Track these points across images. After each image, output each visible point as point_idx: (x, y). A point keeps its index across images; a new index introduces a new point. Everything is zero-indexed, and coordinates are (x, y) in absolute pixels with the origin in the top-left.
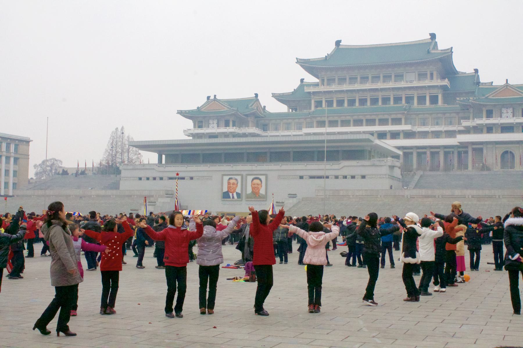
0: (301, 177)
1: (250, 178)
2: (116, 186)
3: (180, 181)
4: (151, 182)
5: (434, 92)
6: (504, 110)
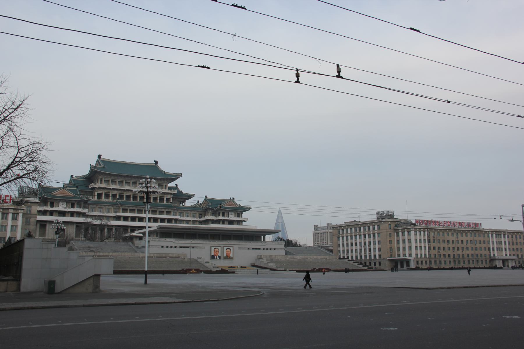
0: (248, 249)
3: (192, 249)
4: (169, 249)
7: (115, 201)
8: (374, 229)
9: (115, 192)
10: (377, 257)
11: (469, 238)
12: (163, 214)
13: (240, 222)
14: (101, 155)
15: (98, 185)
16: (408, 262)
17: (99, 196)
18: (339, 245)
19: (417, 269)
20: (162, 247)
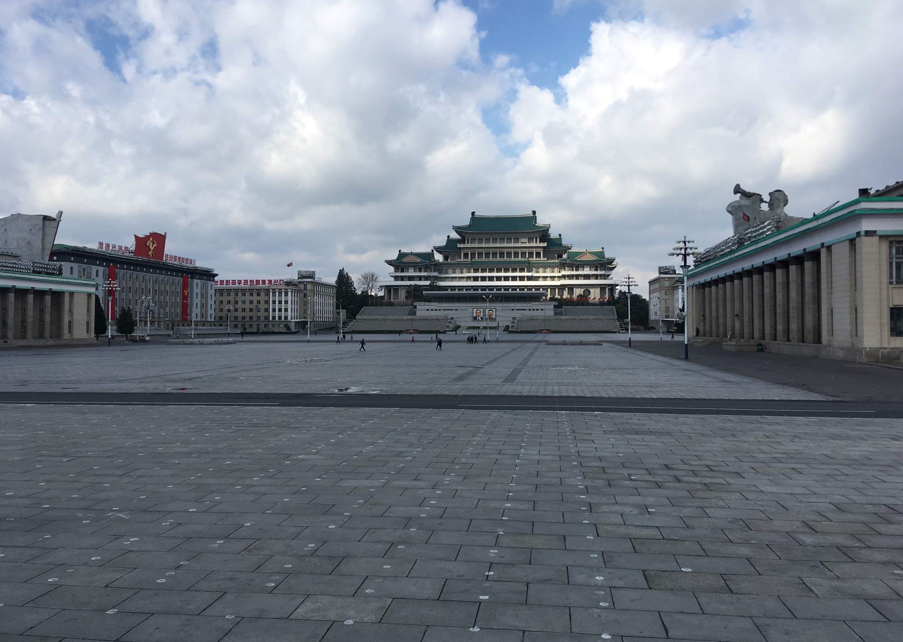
2: (415, 314)
5: (539, 250)
13: (605, 277)
15: (462, 246)
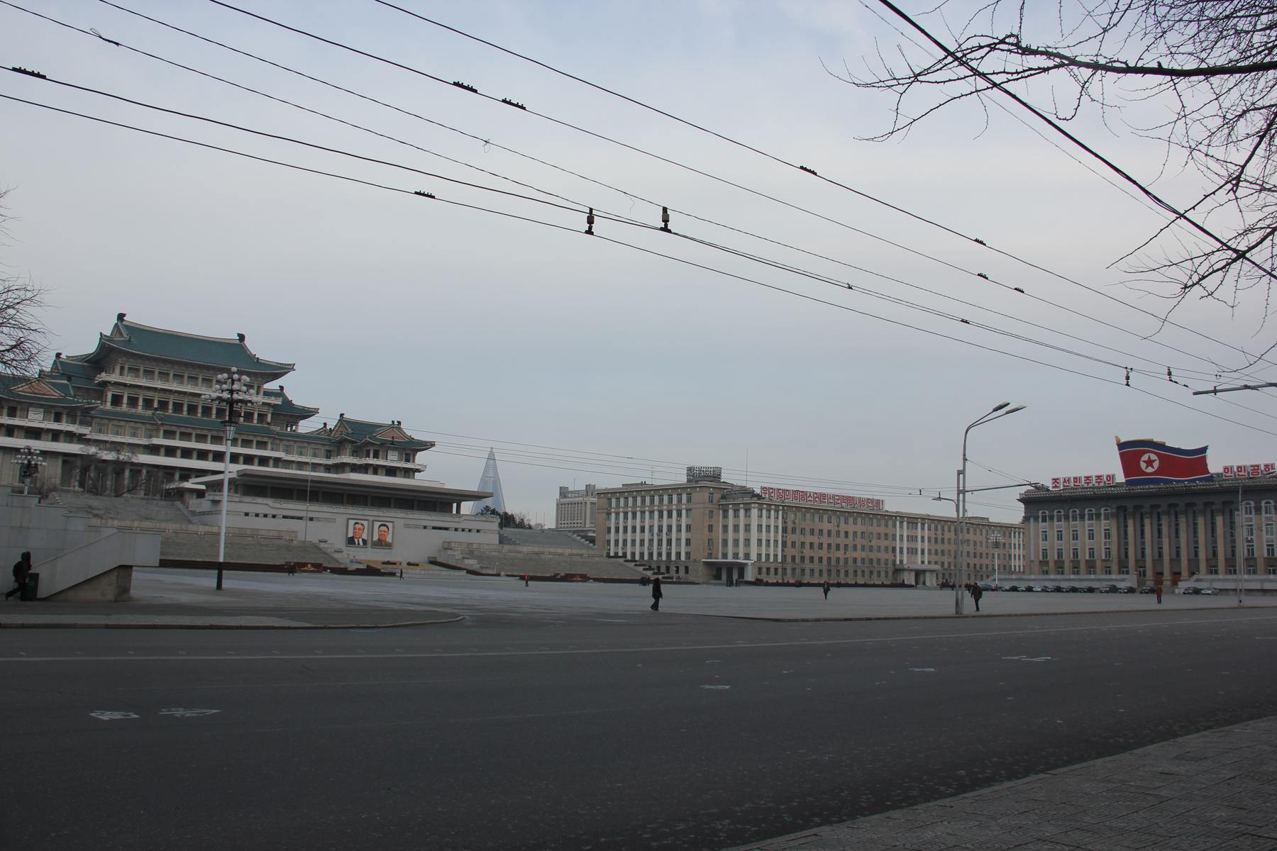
0: (425, 527)
1: (377, 524)
3: (310, 523)
4: (261, 519)
6: (390, 453)
7: (150, 413)
8: (680, 500)
9: (150, 394)
10: (683, 558)
11: (859, 528)
12: (251, 447)
13: (409, 473)
14: (124, 315)
15: (114, 377)
16: (742, 568)
17: (117, 400)
18: (609, 529)
19: (758, 582)
20: (247, 514)
